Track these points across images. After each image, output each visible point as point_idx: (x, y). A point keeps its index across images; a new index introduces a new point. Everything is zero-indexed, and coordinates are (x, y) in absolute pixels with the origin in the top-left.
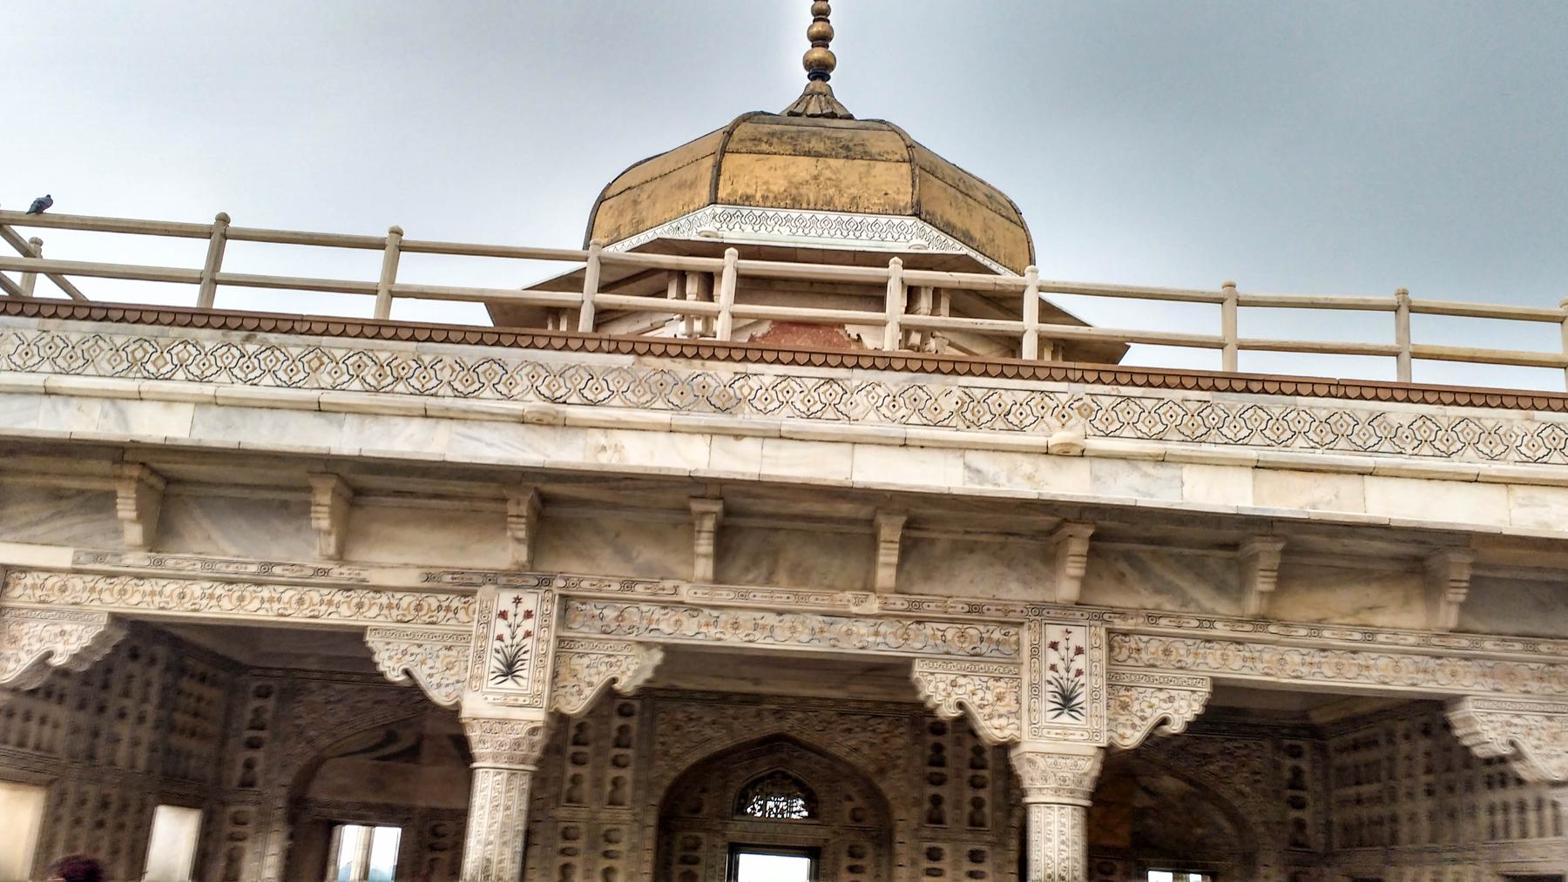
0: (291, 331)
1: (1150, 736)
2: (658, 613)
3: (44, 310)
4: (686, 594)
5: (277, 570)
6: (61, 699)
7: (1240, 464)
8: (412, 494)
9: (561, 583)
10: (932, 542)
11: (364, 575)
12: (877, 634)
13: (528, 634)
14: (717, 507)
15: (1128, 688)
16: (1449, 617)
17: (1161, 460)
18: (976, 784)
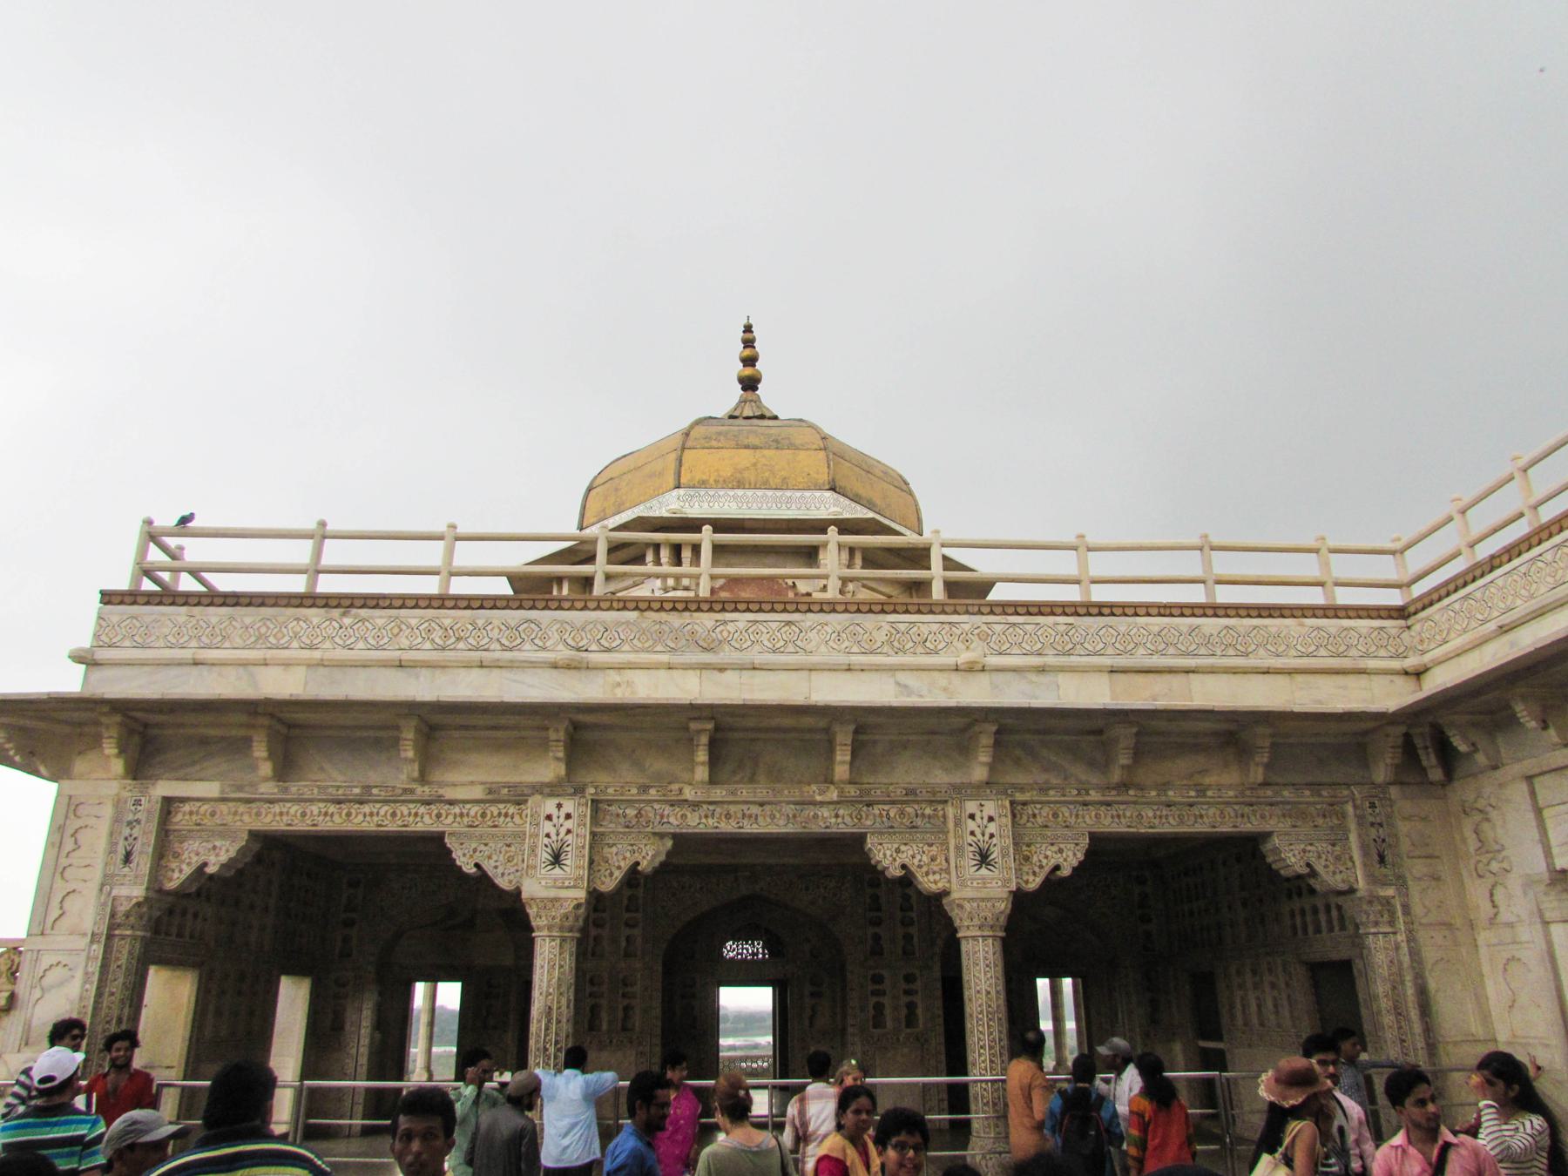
0: (376, 607)
1: (1047, 882)
2: (667, 810)
3: (191, 600)
4: (689, 794)
5: (375, 791)
6: (208, 899)
7: (1099, 670)
8: (474, 727)
9: (592, 791)
10: (875, 742)
11: (441, 792)
12: (837, 816)
13: (569, 831)
14: (710, 726)
15: (1028, 845)
16: (1257, 774)
17: (1042, 670)
18: (906, 923)
